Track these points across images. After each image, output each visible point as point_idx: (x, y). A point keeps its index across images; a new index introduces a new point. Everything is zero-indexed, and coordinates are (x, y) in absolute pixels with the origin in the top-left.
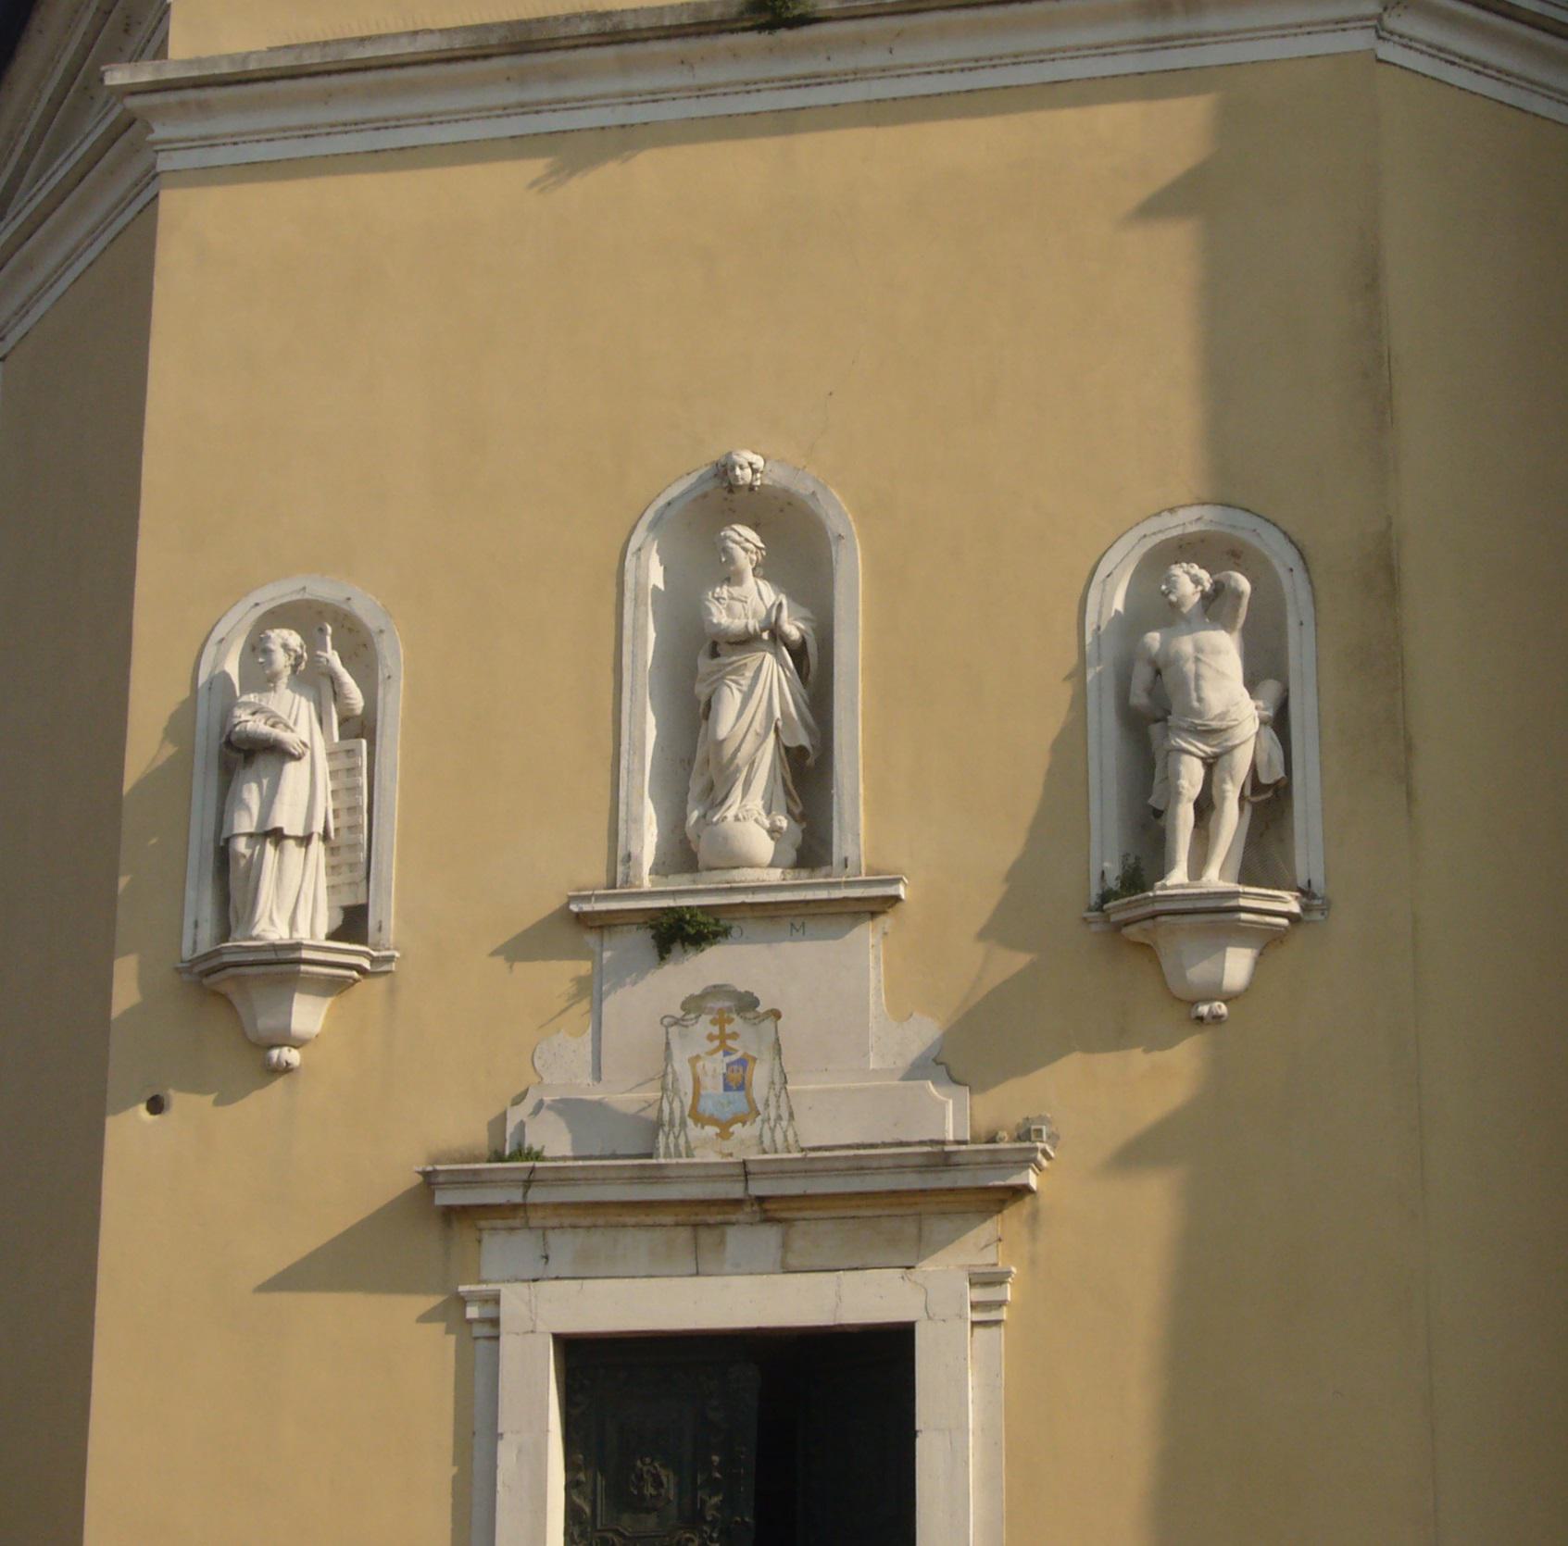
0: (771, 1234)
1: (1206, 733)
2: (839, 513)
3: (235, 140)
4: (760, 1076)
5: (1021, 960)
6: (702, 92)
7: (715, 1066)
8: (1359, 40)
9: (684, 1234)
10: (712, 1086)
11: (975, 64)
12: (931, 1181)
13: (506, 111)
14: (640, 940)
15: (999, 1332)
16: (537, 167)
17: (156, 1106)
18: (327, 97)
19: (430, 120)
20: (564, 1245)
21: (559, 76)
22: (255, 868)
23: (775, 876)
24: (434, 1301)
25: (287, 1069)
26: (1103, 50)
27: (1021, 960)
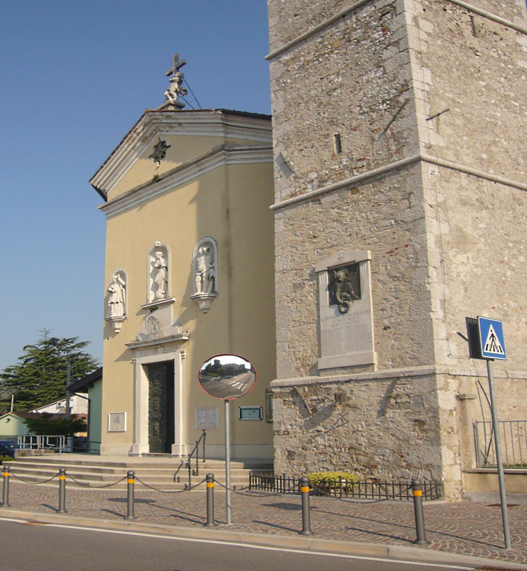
0: (162, 348)
1: (200, 272)
2: (169, 248)
3: (113, 212)
4: (157, 327)
5: (186, 308)
6: (155, 192)
7: (152, 327)
8: (223, 163)
9: (154, 349)
10: (153, 330)
11: (181, 180)
12: (172, 340)
13: (136, 201)
14: (149, 311)
15: (185, 360)
16: (138, 209)
17: (108, 339)
18: (120, 204)
19: (130, 204)
20: (143, 352)
21: (140, 194)
22: (111, 308)
23: (164, 299)
24: (131, 361)
25: (118, 333)
26: (194, 173)
27: (186, 308)
